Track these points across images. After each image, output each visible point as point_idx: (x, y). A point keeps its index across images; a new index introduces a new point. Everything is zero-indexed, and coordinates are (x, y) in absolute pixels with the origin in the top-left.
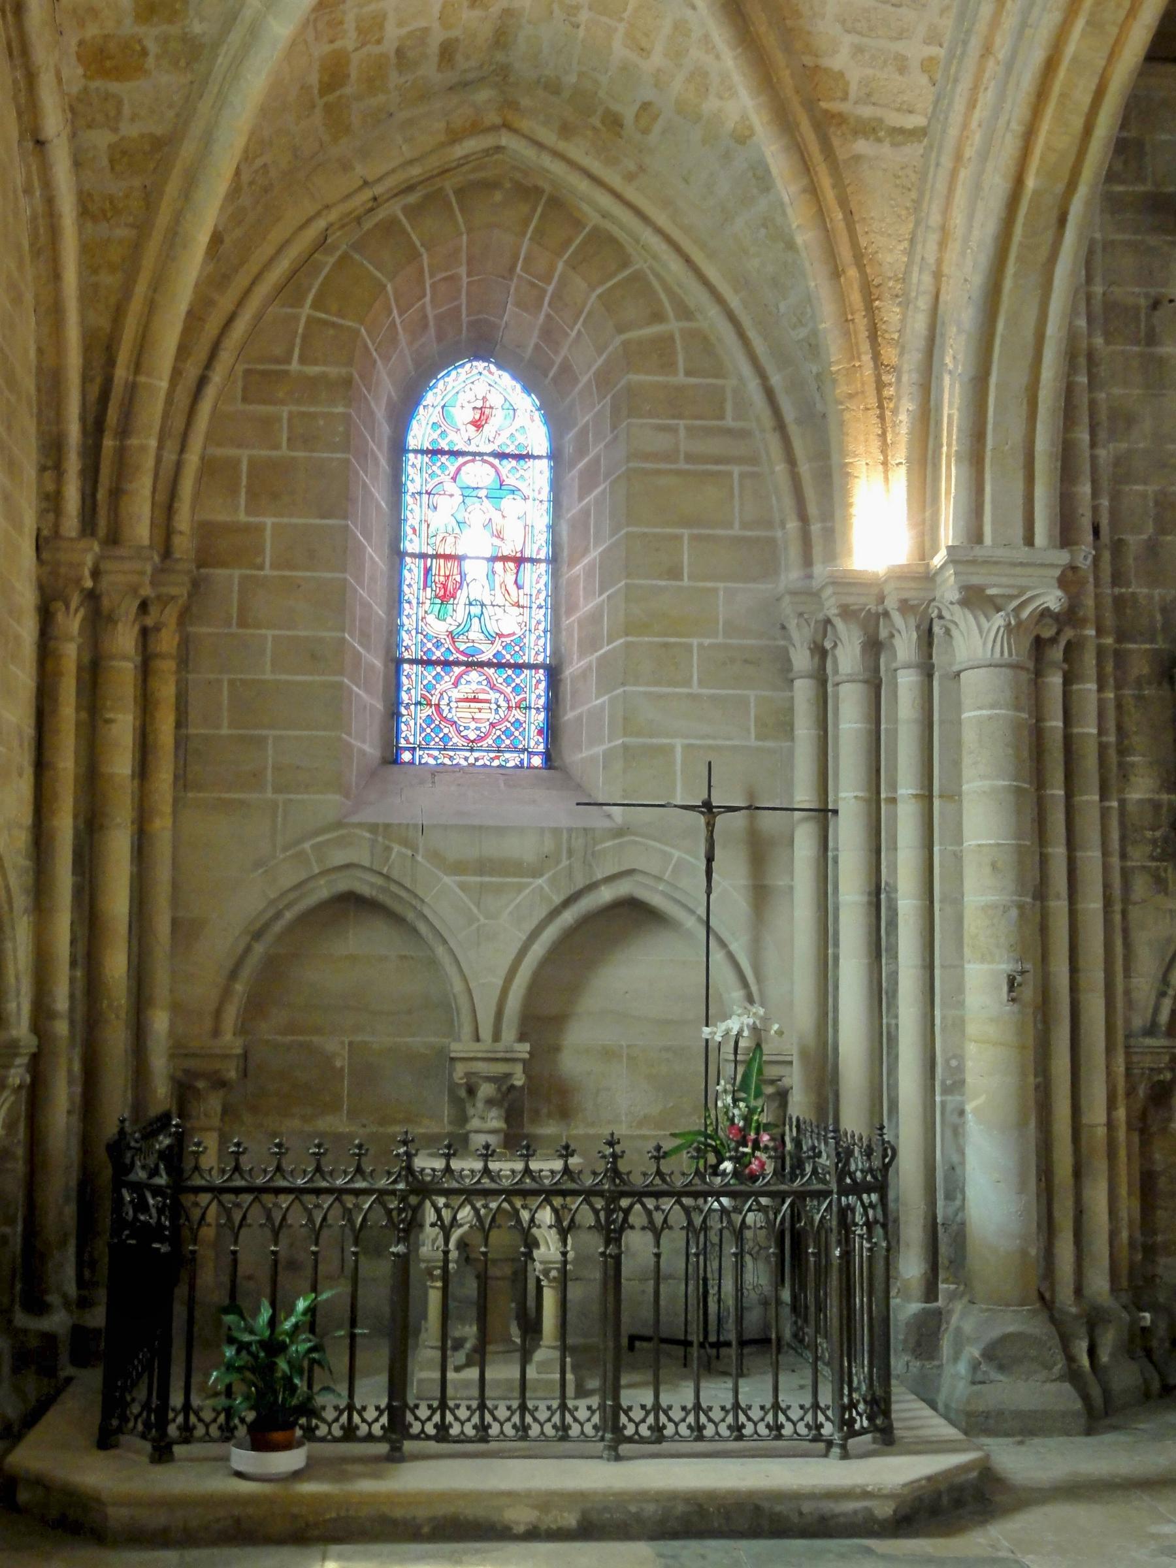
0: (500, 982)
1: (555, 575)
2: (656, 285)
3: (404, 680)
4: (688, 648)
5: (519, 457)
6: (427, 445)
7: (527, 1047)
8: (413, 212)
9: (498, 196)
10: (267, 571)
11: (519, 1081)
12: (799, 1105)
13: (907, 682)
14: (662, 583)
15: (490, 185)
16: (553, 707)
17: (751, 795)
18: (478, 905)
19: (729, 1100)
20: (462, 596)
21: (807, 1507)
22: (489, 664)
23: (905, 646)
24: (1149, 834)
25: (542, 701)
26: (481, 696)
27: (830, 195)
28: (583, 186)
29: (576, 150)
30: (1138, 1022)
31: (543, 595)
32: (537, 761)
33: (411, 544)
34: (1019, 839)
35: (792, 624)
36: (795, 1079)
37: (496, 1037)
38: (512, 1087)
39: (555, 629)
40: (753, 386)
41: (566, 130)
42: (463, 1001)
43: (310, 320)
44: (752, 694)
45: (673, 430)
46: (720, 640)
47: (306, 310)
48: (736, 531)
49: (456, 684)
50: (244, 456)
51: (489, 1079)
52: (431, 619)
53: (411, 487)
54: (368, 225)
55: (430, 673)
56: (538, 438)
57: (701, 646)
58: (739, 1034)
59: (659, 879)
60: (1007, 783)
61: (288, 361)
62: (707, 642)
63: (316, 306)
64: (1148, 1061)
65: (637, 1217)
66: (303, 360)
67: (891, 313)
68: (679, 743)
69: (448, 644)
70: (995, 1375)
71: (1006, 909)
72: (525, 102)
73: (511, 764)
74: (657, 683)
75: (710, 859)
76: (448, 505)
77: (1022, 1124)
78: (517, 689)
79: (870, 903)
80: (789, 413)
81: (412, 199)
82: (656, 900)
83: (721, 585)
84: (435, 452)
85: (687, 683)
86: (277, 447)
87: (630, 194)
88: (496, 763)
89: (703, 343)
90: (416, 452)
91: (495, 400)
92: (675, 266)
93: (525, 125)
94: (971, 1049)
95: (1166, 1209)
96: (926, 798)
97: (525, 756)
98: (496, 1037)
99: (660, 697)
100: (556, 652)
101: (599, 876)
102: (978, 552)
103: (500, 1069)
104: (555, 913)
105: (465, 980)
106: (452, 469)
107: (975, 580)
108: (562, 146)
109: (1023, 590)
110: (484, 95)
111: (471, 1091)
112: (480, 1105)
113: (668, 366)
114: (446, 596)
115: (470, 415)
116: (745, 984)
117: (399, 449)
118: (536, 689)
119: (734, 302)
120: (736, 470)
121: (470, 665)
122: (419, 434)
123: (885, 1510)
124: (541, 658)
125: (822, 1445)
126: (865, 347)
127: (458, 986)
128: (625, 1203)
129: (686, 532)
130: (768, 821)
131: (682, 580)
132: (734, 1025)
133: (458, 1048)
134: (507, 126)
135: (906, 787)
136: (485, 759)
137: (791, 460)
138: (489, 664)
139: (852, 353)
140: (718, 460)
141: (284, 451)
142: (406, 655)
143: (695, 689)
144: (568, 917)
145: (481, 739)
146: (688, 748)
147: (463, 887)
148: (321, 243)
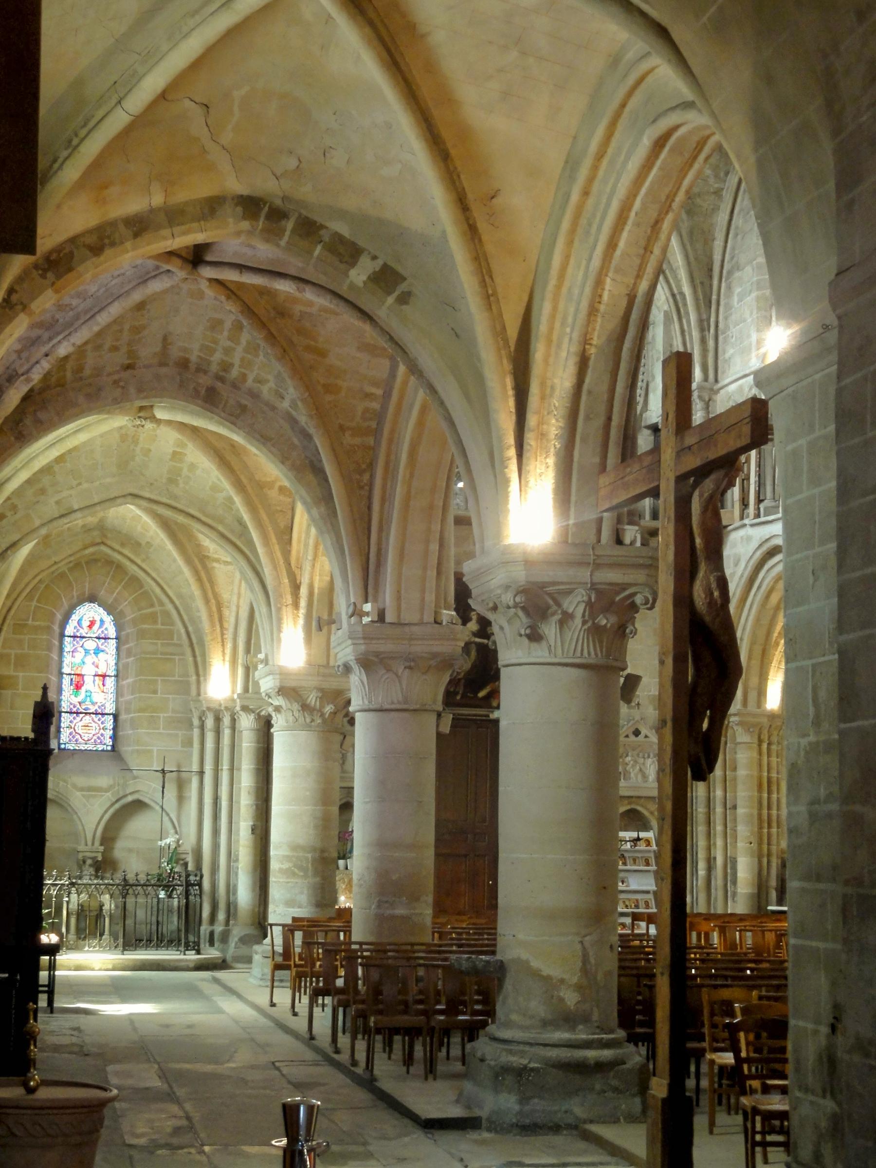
0: (94, 827)
1: (117, 681)
2: (152, 594)
3: (62, 719)
4: (159, 717)
5: (105, 639)
6: (72, 635)
7: (102, 847)
8: (71, 570)
9: (100, 564)
10: (20, 691)
11: (100, 859)
12: (190, 867)
13: (226, 733)
15: (96, 561)
16: (115, 729)
17: (179, 766)
18: (88, 801)
19: (166, 864)
20: (83, 689)
21: (172, 964)
22: (93, 714)
23: (226, 721)
25: (112, 727)
26: (90, 725)
27: (205, 579)
28: (128, 563)
29: (126, 552)
31: (113, 688)
32: (109, 748)
33: (66, 670)
35: (193, 710)
36: (190, 859)
37: (93, 844)
38: (98, 861)
39: (117, 702)
40: (183, 631)
41: (123, 545)
42: (83, 835)
43: (36, 607)
44: (180, 733)
45: (156, 644)
46: (170, 714)
47: (34, 603)
48: (176, 678)
49: (81, 720)
50: (13, 652)
51: (91, 858)
52: (73, 697)
53: (66, 649)
54: (56, 574)
55: (71, 717)
56: (112, 632)
57: (164, 717)
58: (170, 844)
59: (147, 793)
61: (27, 620)
62: (165, 715)
63: (38, 601)
65: (130, 891)
66: (33, 620)
67: (226, 612)
68: (155, 749)
69: (78, 706)
70: (241, 945)
71: (252, 806)
72: (109, 535)
73: (100, 749)
75: (163, 788)
76: (80, 655)
77: (255, 870)
78: (102, 723)
79: (214, 803)
80: (194, 641)
81: (71, 565)
82: (146, 800)
83: (170, 696)
84: (74, 637)
85: (158, 729)
86: (23, 649)
87: (144, 566)
88: (94, 749)
89: (167, 614)
90: (69, 636)
91: (97, 619)
92: (158, 590)
93: (109, 542)
94: (241, 849)
96: (232, 770)
97: (105, 746)
98: (93, 844)
100: (117, 709)
101: (128, 792)
102: (247, 695)
103: (94, 855)
104: (113, 804)
105: (83, 825)
106: (81, 643)
107: (246, 704)
108: (121, 550)
110: (96, 533)
111: (84, 862)
112: (87, 866)
113: (155, 622)
114: (78, 687)
115: (88, 623)
116: (175, 827)
117: (62, 635)
118: (109, 722)
119: (177, 602)
120: (177, 657)
121: (86, 713)
122: (70, 630)
123: (192, 965)
124: (111, 712)
125: (179, 952)
126: (217, 623)
127: (80, 828)
128: (127, 887)
129: (159, 678)
130: (184, 775)
132: (168, 841)
133: (81, 848)
134: (103, 543)
135: (225, 766)
136: (91, 747)
137: (194, 656)
138: (93, 714)
139: (213, 625)
140: (171, 654)
141: (26, 651)
142: (63, 710)
143: (161, 731)
144: (117, 806)
145: (88, 740)
146: (158, 750)
147: (84, 796)
148: (40, 581)
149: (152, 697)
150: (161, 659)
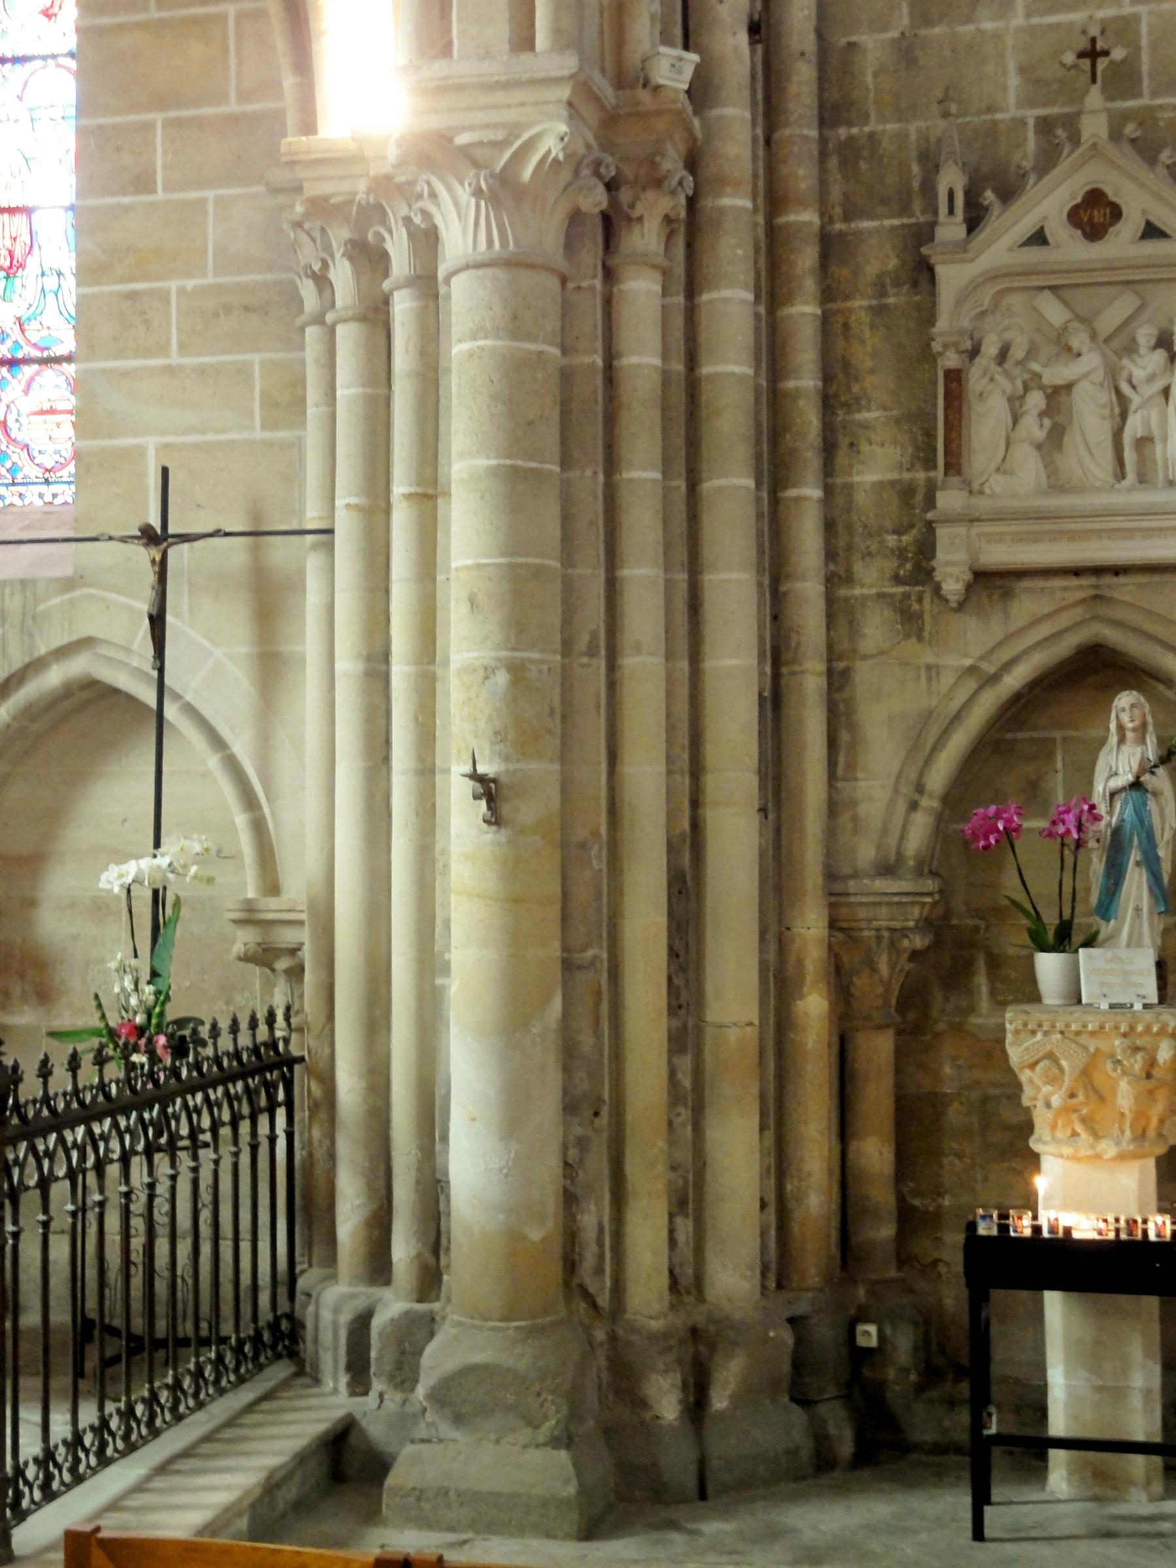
4: (164, 296)
14: (127, 200)
17: (256, 515)
20: (32, 264)
24: (891, 540)
30: (866, 853)
34: (512, 554)
44: (256, 359)
49: (26, 392)
57: (182, 291)
60: (493, 462)
62: (190, 284)
64: (883, 918)
69: (16, 334)
70: (446, 1430)
71: (488, 672)
74: (120, 354)
83: (210, 194)
85: (162, 349)
95: (959, 1156)
99: (125, 374)
101: (42, 650)
109: (515, 130)
130: (279, 552)
131: (154, 191)
143: (175, 359)
149: (128, 209)
150: (160, 25)
